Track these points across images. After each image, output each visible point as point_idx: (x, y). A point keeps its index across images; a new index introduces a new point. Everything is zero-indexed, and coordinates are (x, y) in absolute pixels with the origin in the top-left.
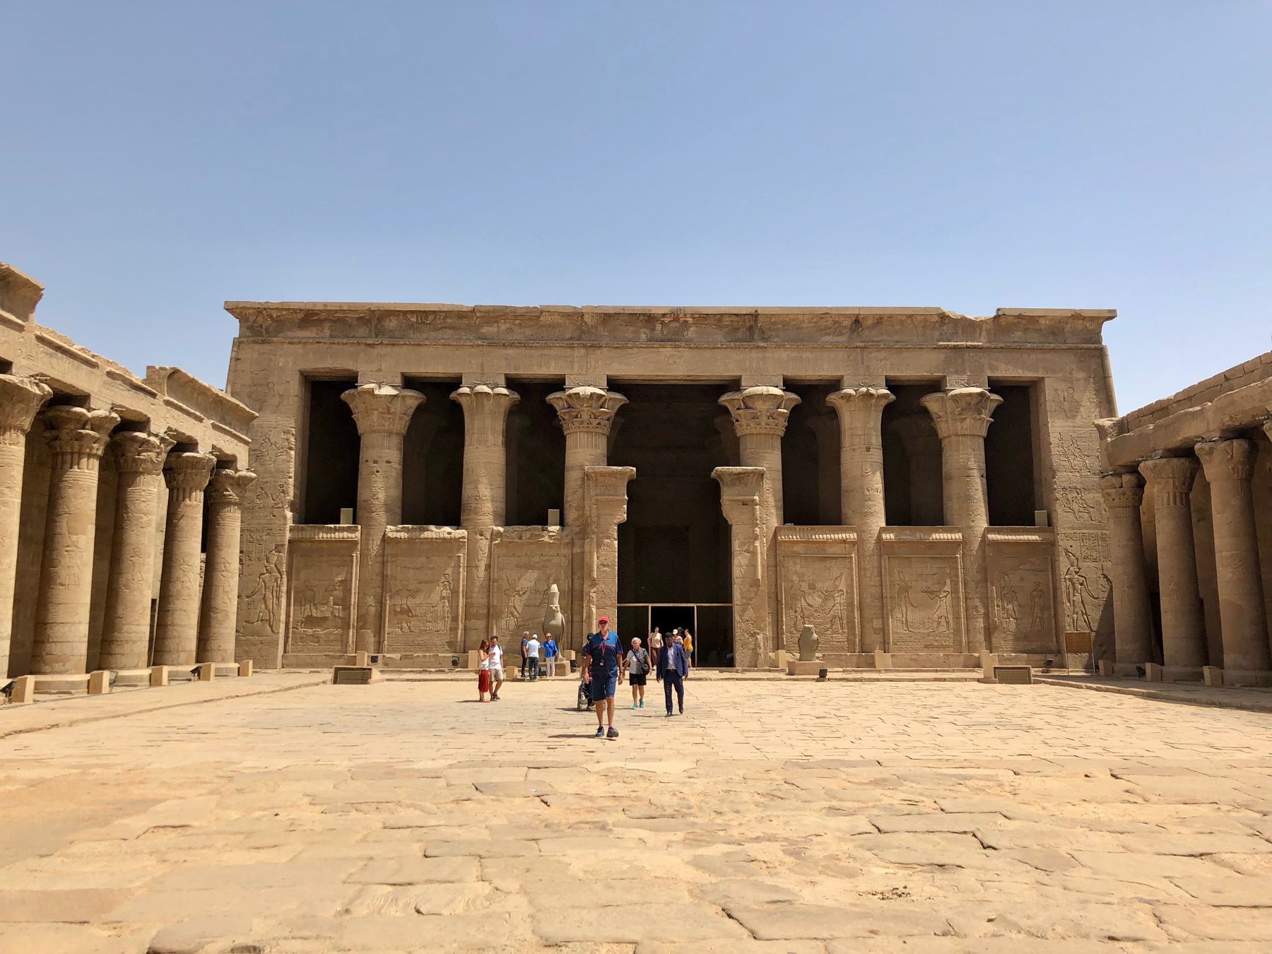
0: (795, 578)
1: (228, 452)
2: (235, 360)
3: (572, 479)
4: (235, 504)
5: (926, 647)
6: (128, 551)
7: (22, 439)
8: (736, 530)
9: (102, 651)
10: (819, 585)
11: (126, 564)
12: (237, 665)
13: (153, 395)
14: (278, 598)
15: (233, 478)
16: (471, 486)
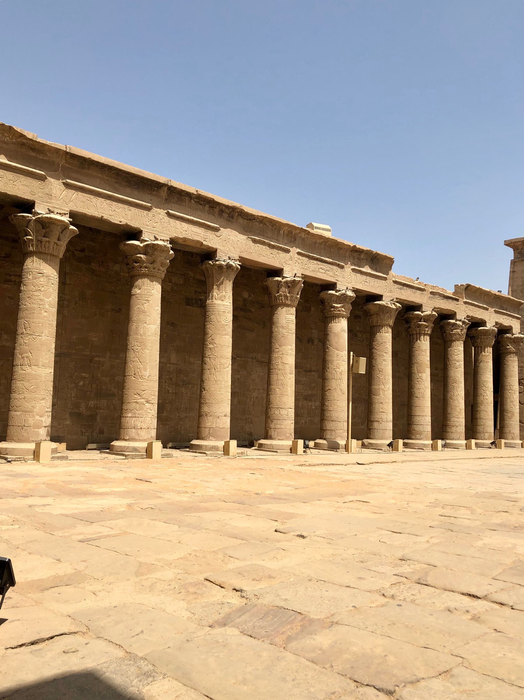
1: (506, 325)
2: (512, 272)
4: (513, 353)
6: (450, 380)
7: (390, 330)
9: (440, 430)
11: (450, 387)
12: (521, 442)
13: (457, 300)
15: (511, 338)
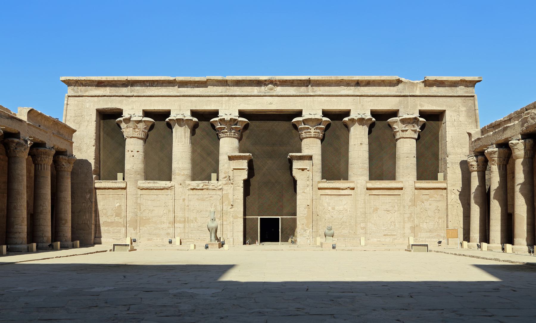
0: (326, 205)
3: (223, 159)
5: (385, 235)
8: (298, 183)
10: (337, 208)
14: (91, 213)
16: (176, 163)
